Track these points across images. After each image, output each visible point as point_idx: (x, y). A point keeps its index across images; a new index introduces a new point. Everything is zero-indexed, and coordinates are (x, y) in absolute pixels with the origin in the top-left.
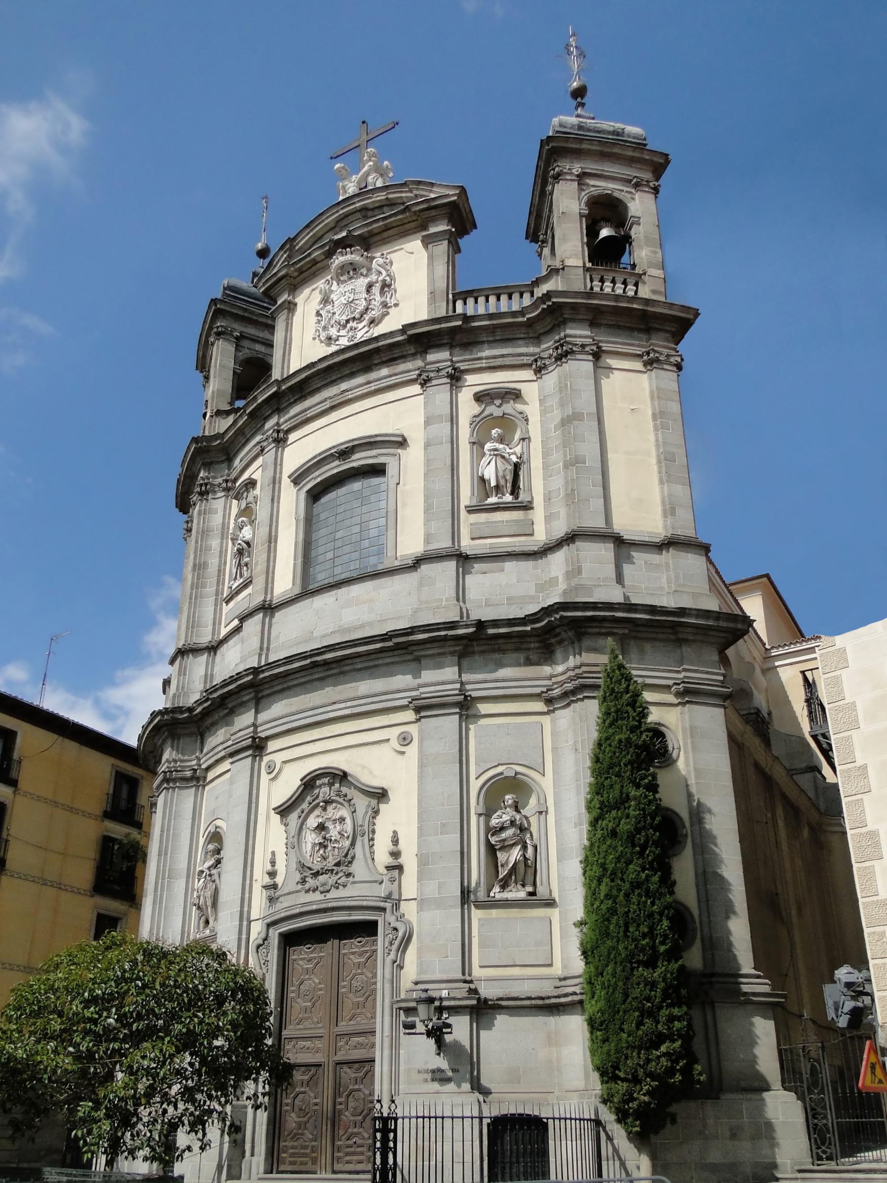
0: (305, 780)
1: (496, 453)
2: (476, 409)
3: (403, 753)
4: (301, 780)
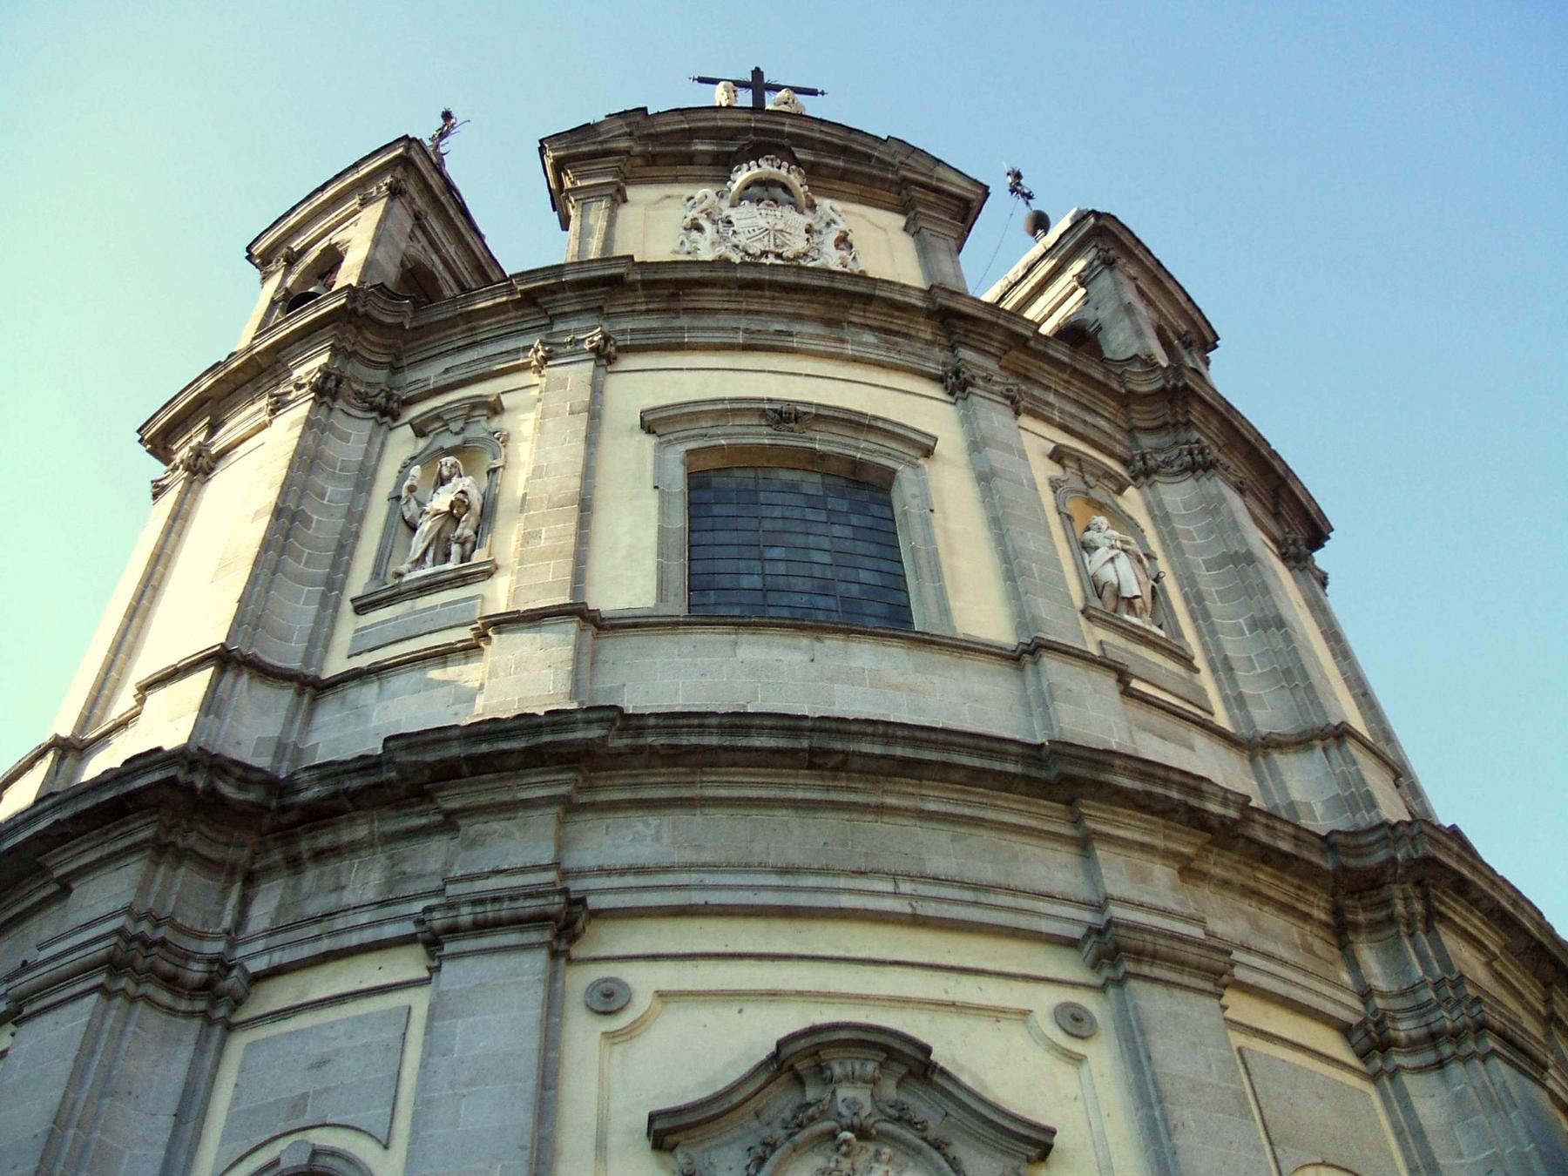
0: (786, 1052)
1: (1127, 547)
2: (1056, 471)
3: (1077, 1059)
4: (781, 1044)
